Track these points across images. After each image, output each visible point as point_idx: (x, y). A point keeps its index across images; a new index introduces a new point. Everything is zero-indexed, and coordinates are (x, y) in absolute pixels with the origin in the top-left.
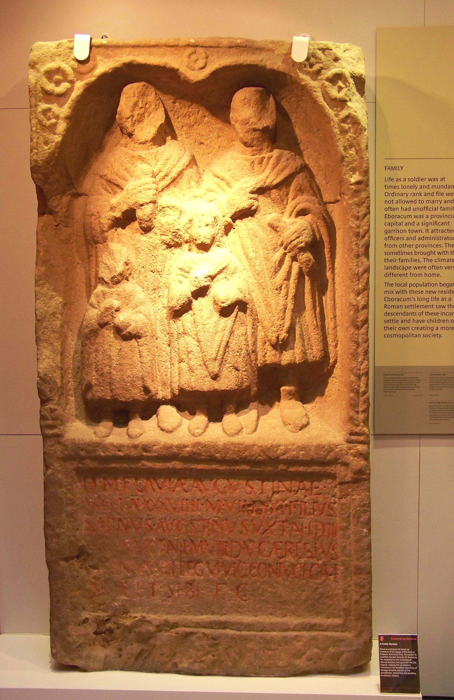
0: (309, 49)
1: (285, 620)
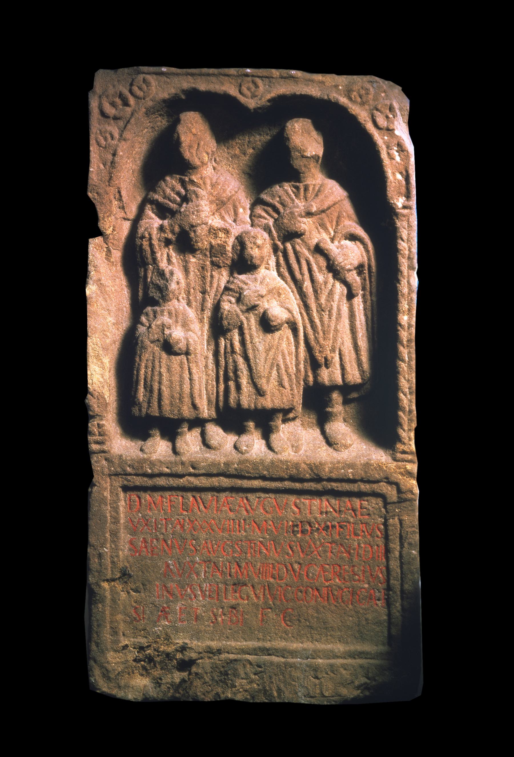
1: (329, 646)
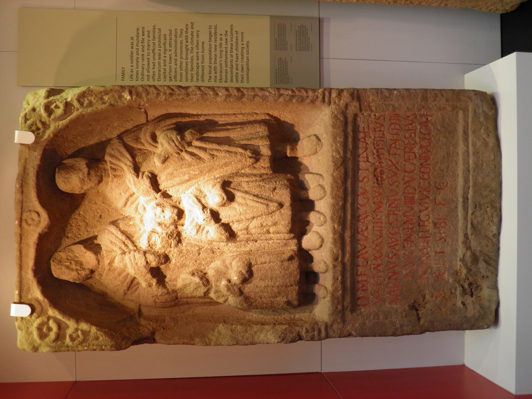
0: (25, 130)
1: (461, 154)
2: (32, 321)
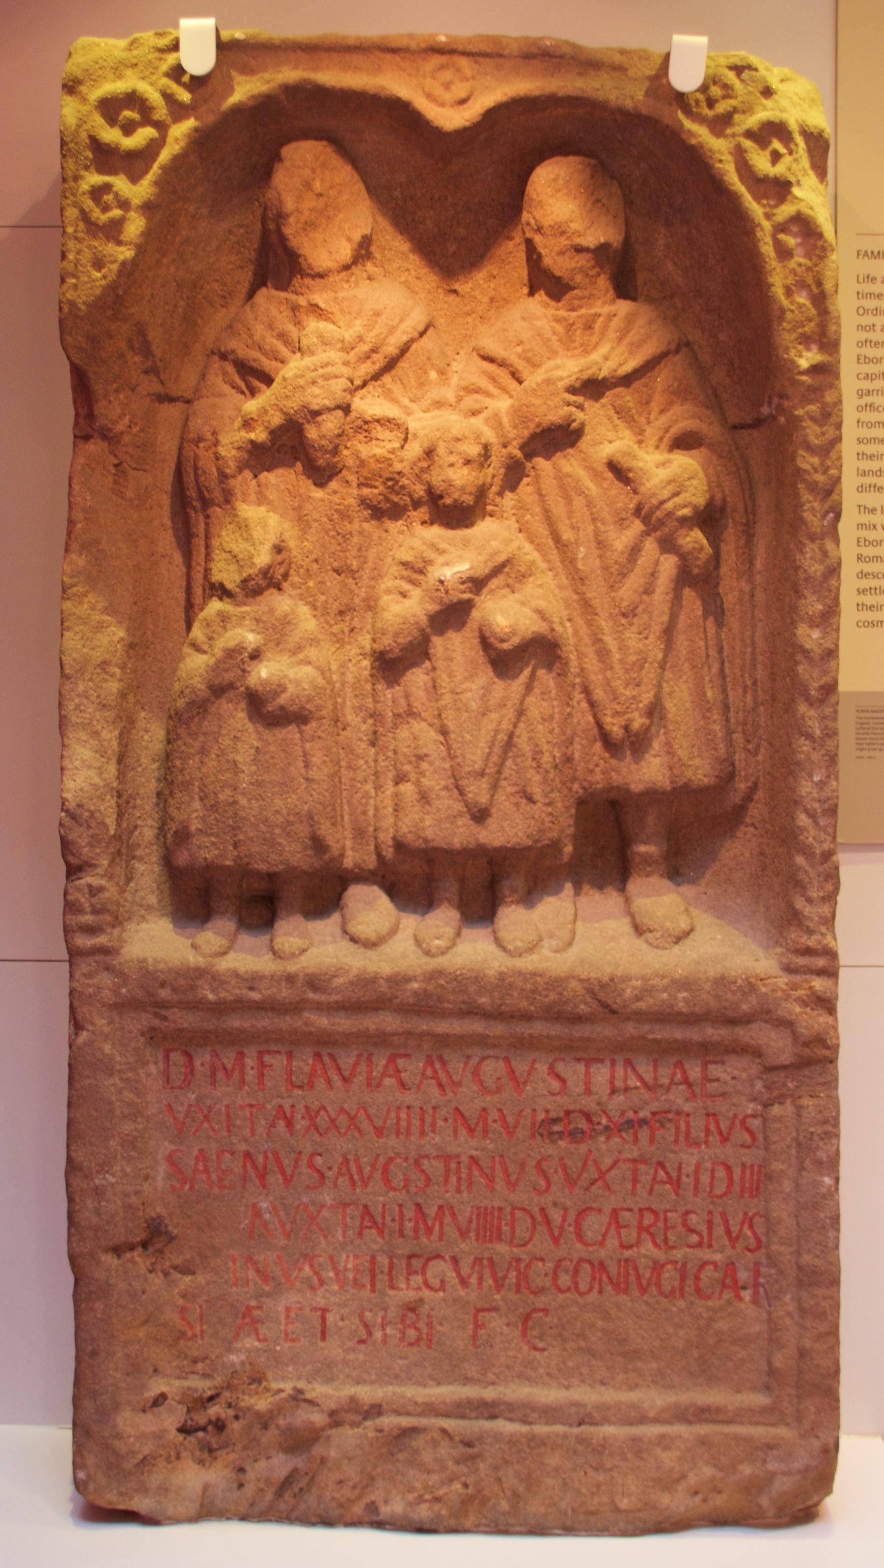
0: (708, 67)
1: (633, 1396)
2: (154, 77)
